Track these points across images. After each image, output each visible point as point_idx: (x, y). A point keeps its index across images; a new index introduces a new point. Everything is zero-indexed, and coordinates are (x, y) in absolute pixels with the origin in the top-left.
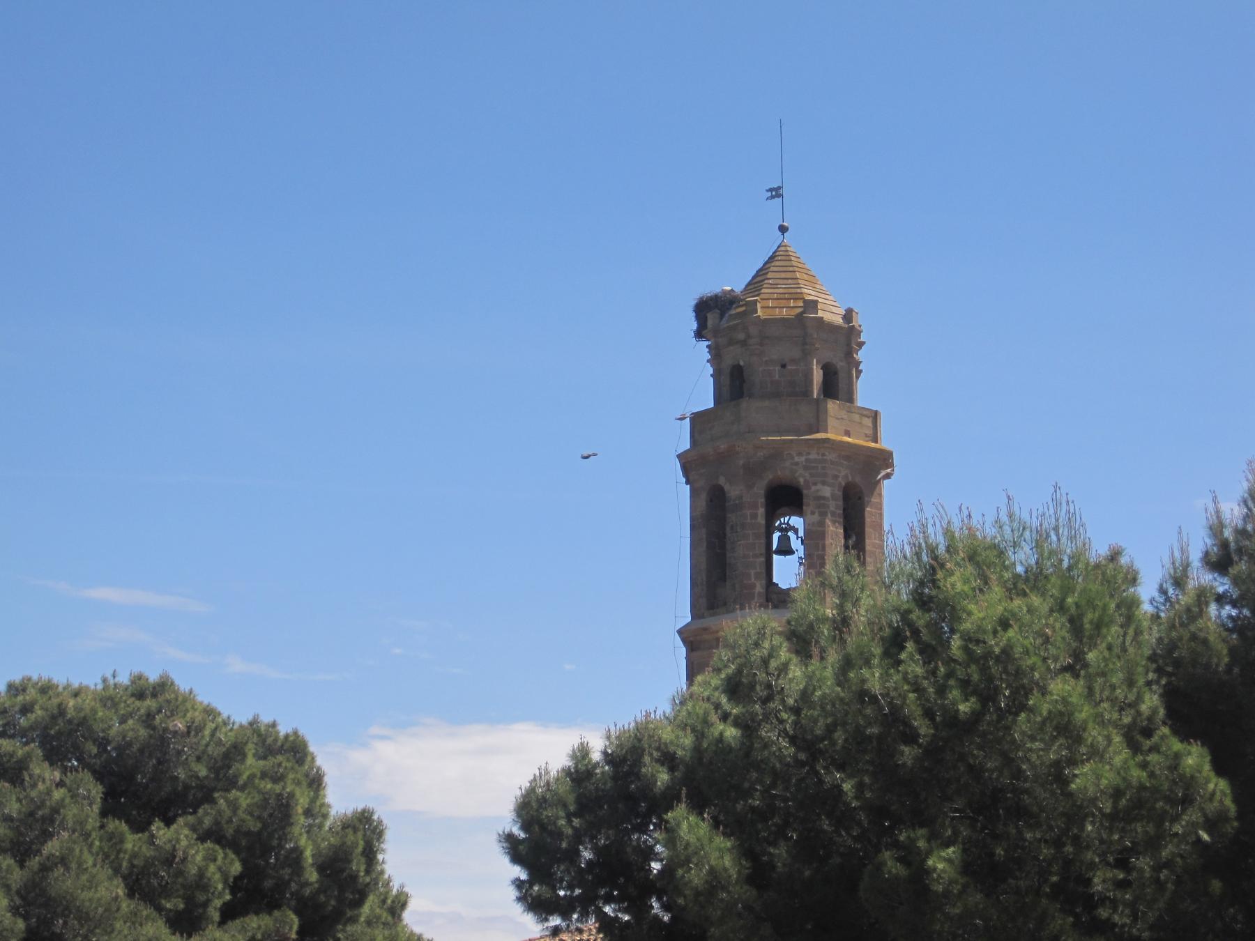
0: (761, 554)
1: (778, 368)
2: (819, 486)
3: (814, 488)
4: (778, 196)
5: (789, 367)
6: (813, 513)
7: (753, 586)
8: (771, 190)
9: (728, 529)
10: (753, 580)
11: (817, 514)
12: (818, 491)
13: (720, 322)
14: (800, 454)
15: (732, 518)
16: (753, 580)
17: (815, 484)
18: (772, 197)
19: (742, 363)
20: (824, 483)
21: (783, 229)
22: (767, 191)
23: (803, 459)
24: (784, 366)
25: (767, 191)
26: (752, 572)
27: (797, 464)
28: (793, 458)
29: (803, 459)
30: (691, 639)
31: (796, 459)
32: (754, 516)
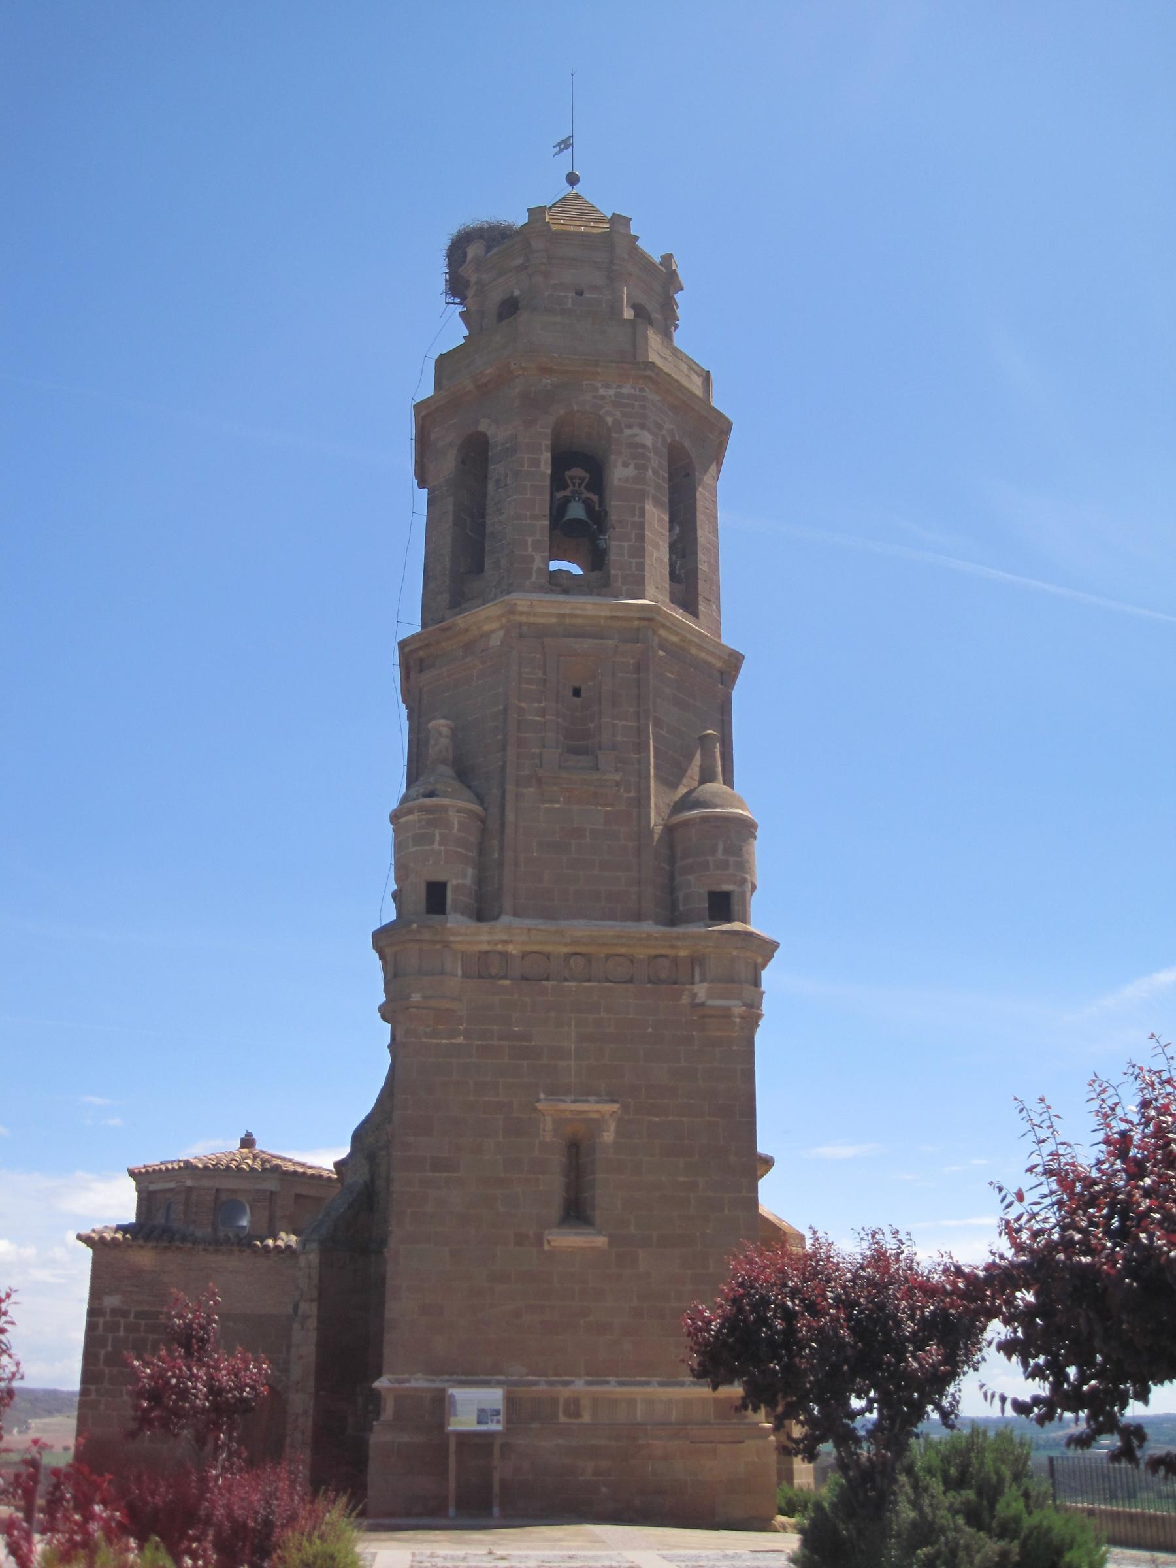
0: (545, 516)
1: (571, 295)
2: (636, 430)
3: (627, 432)
4: (566, 147)
5: (587, 295)
6: (626, 465)
7: (532, 559)
8: (559, 144)
9: (491, 486)
10: (530, 550)
11: (632, 467)
12: (635, 435)
13: (487, 252)
14: (607, 386)
15: (496, 470)
16: (530, 550)
17: (630, 427)
18: (561, 151)
19: (517, 293)
20: (643, 426)
21: (572, 179)
22: (554, 147)
23: (612, 392)
24: (580, 293)
25: (554, 147)
26: (530, 540)
27: (603, 398)
28: (597, 389)
29: (612, 392)
30: (421, 653)
31: (602, 392)
32: (536, 463)
